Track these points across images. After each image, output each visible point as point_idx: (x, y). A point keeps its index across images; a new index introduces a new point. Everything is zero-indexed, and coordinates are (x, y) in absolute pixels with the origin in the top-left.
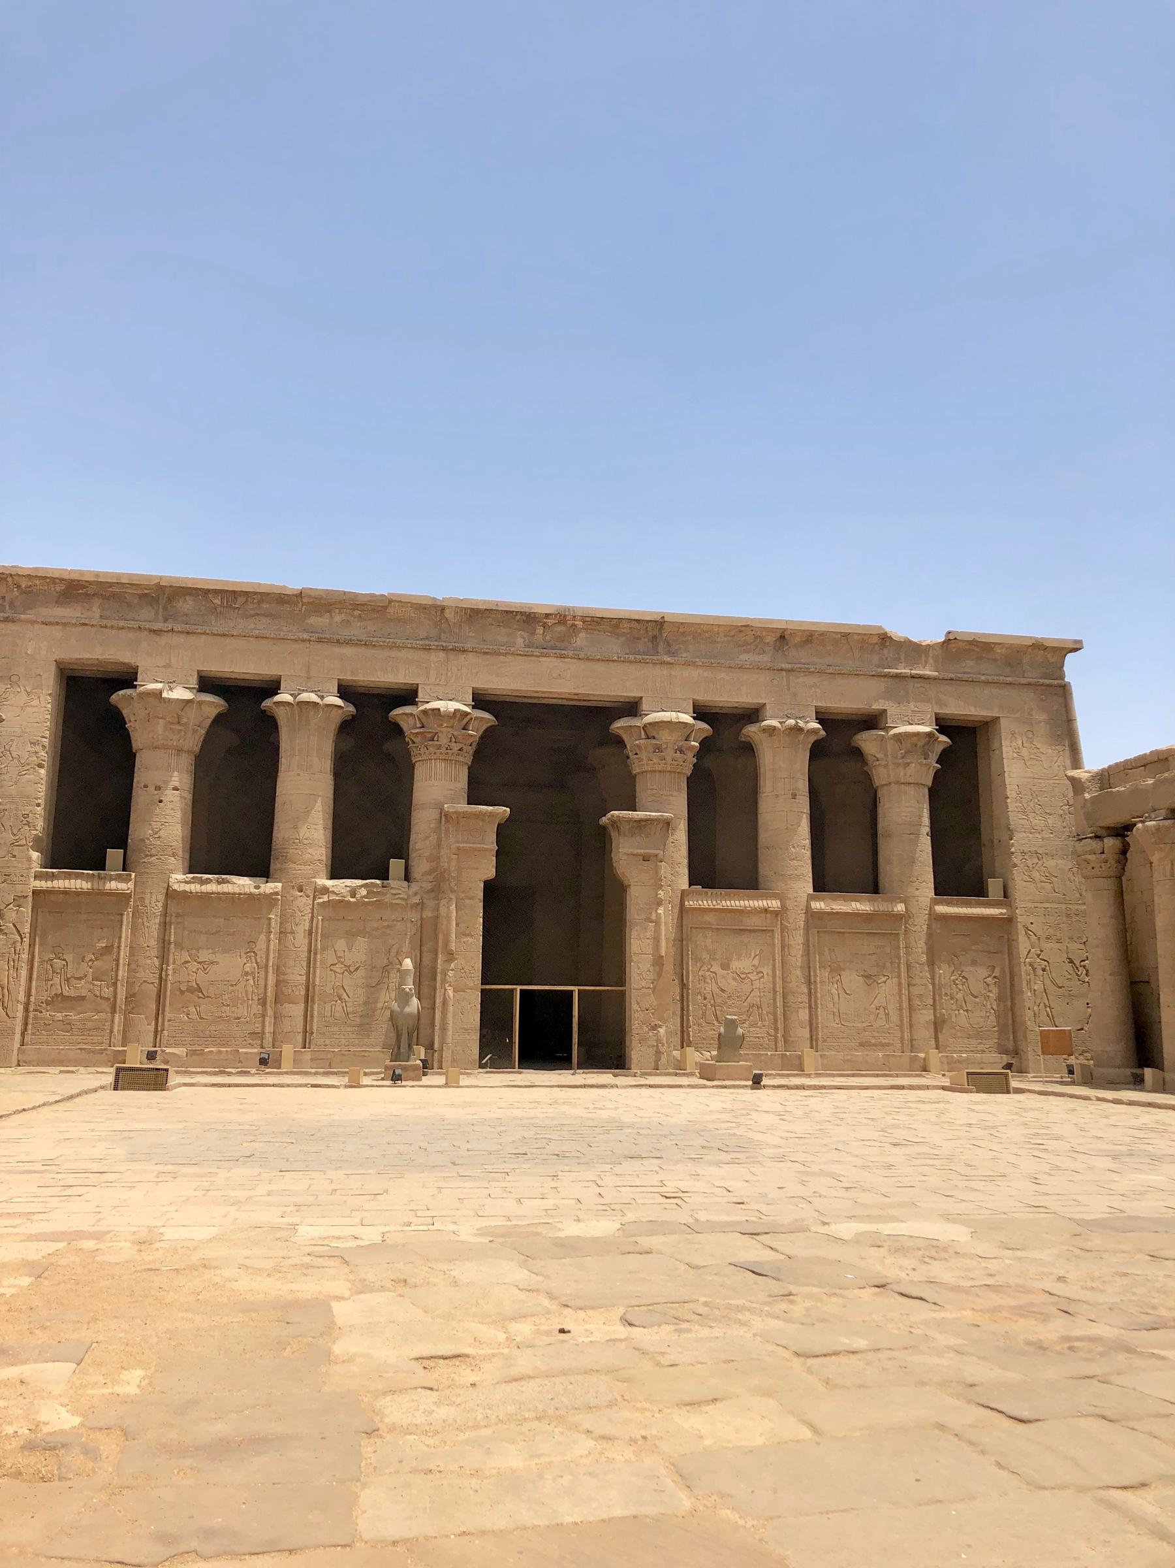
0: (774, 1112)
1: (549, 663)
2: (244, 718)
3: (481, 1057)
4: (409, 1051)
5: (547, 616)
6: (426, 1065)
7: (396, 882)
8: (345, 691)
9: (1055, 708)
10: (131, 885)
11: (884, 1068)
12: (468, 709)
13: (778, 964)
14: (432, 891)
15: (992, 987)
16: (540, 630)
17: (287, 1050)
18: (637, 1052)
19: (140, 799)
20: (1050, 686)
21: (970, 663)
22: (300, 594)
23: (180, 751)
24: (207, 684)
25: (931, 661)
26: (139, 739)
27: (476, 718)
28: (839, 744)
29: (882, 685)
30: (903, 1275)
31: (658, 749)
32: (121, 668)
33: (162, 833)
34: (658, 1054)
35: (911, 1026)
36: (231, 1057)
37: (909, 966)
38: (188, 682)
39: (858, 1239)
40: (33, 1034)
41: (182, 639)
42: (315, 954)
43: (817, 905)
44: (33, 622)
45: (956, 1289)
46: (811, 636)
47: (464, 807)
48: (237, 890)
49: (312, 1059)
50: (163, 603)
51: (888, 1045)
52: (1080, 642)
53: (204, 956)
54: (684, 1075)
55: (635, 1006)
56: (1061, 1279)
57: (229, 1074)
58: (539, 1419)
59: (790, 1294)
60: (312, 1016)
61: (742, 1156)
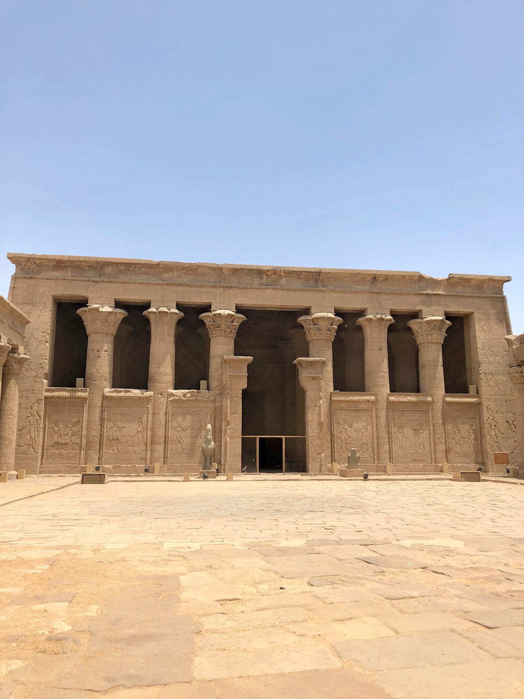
0: (374, 491)
2: (135, 319)
3: (242, 467)
4: (210, 465)
5: (268, 271)
6: (218, 471)
7: (203, 391)
8: (179, 306)
9: (499, 307)
10: (87, 394)
11: (423, 471)
12: (234, 313)
13: (374, 425)
14: (218, 394)
15: (471, 434)
16: (265, 277)
17: (157, 465)
18: (311, 465)
20: (496, 297)
21: (460, 288)
22: (159, 264)
23: (107, 334)
24: (118, 304)
25: (442, 287)
26: (89, 330)
27: (237, 317)
28: (401, 326)
29: (420, 298)
30: (434, 563)
31: (319, 329)
32: (81, 298)
33: (100, 371)
34: (321, 465)
35: (435, 452)
36: (132, 469)
37: (434, 425)
38: (110, 304)
39: (413, 547)
40: (46, 460)
41: (107, 285)
42: (168, 423)
43: (392, 398)
44: (42, 279)
45: (458, 569)
46: (388, 277)
47: (233, 357)
48: (133, 395)
49: (168, 469)
50: (98, 269)
51: (425, 460)
52: (510, 277)
53: (120, 424)
54: (333, 475)
55: (310, 444)
56: (506, 565)
57: (132, 476)
58: (272, 627)
59: (383, 572)
60: (167, 450)
61: (360, 511)
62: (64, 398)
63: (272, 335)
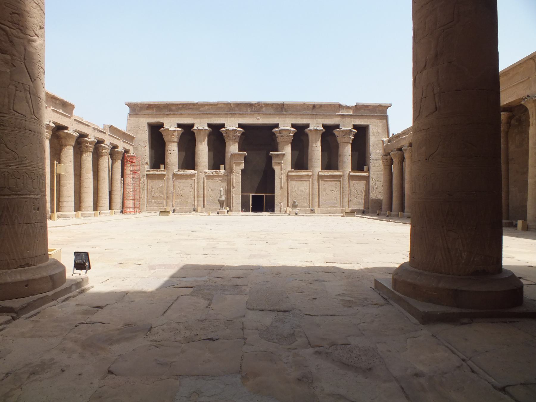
7: (222, 171)
19: (167, 153)
63: (259, 140)
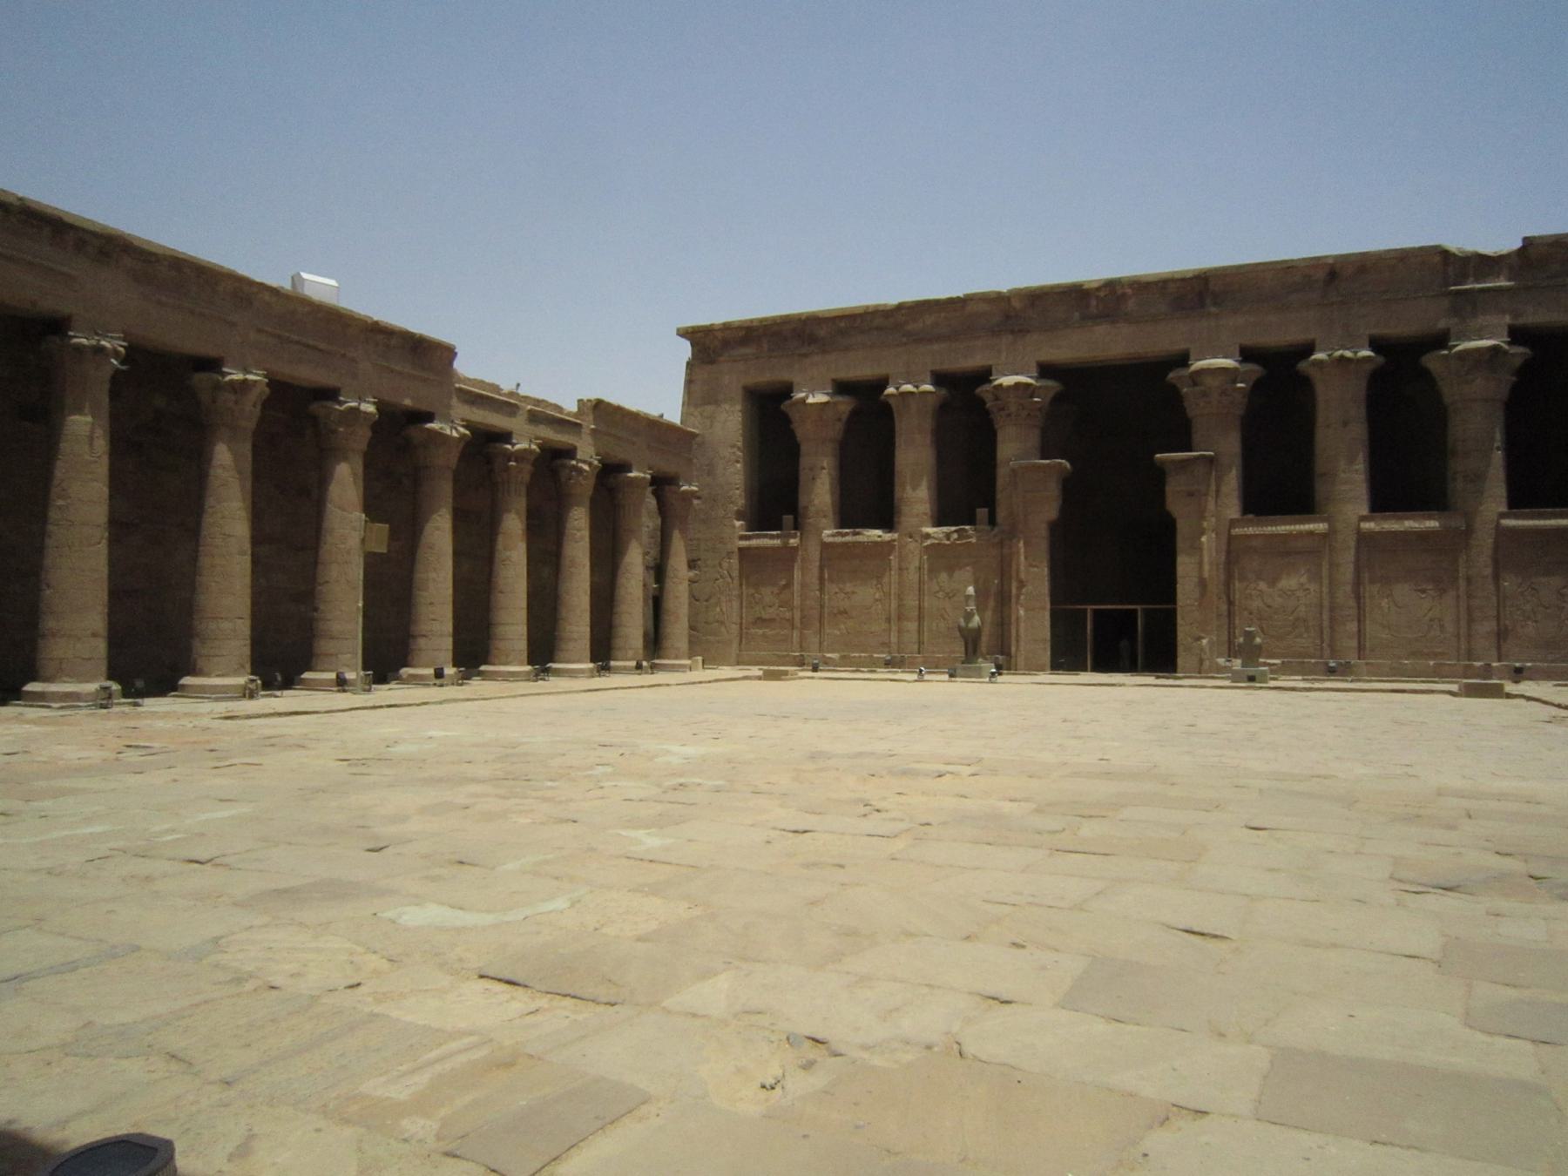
1: (1101, 330)
5: (1098, 289)
8: (939, 379)
12: (1029, 381)
13: (1326, 582)
19: (804, 476)
22: (900, 307)
24: (841, 388)
35: (1469, 635)
37: (1469, 580)
43: (1366, 526)
51: (1442, 654)
62: (766, 548)
